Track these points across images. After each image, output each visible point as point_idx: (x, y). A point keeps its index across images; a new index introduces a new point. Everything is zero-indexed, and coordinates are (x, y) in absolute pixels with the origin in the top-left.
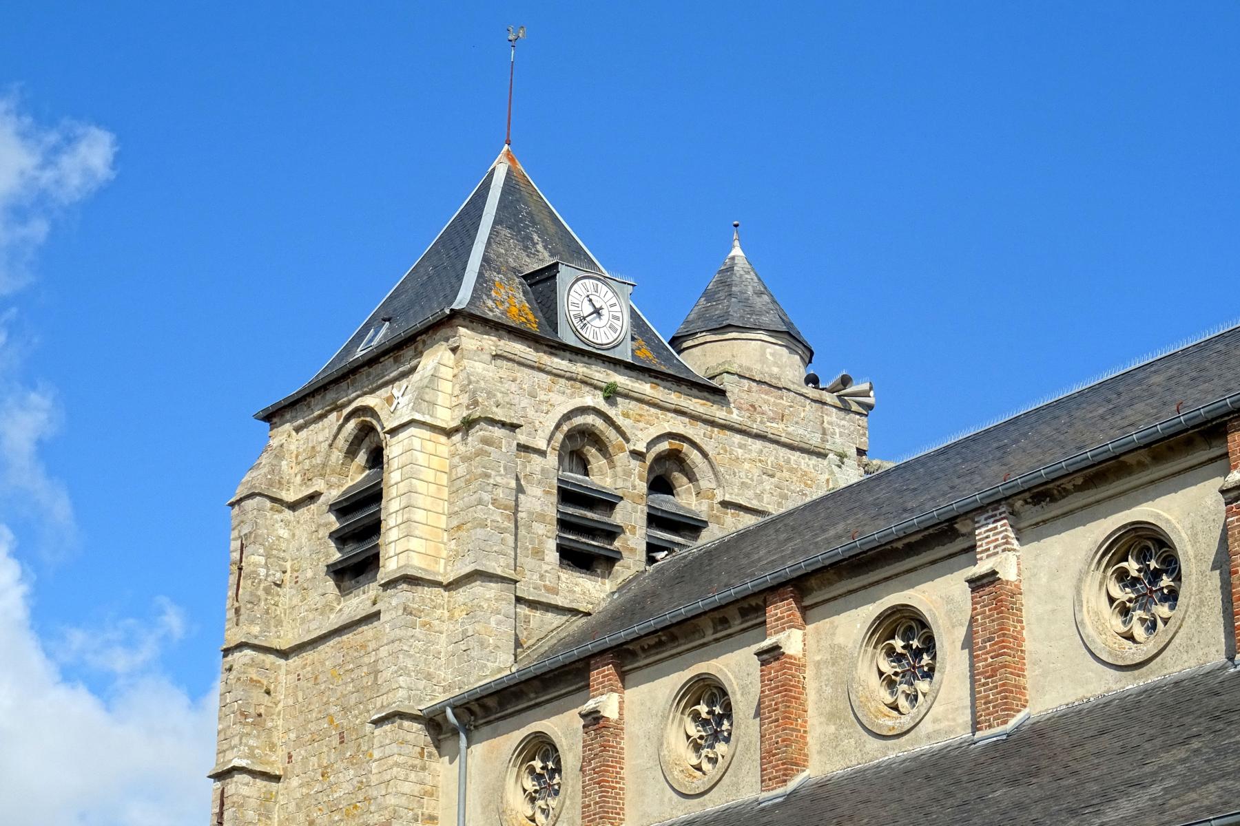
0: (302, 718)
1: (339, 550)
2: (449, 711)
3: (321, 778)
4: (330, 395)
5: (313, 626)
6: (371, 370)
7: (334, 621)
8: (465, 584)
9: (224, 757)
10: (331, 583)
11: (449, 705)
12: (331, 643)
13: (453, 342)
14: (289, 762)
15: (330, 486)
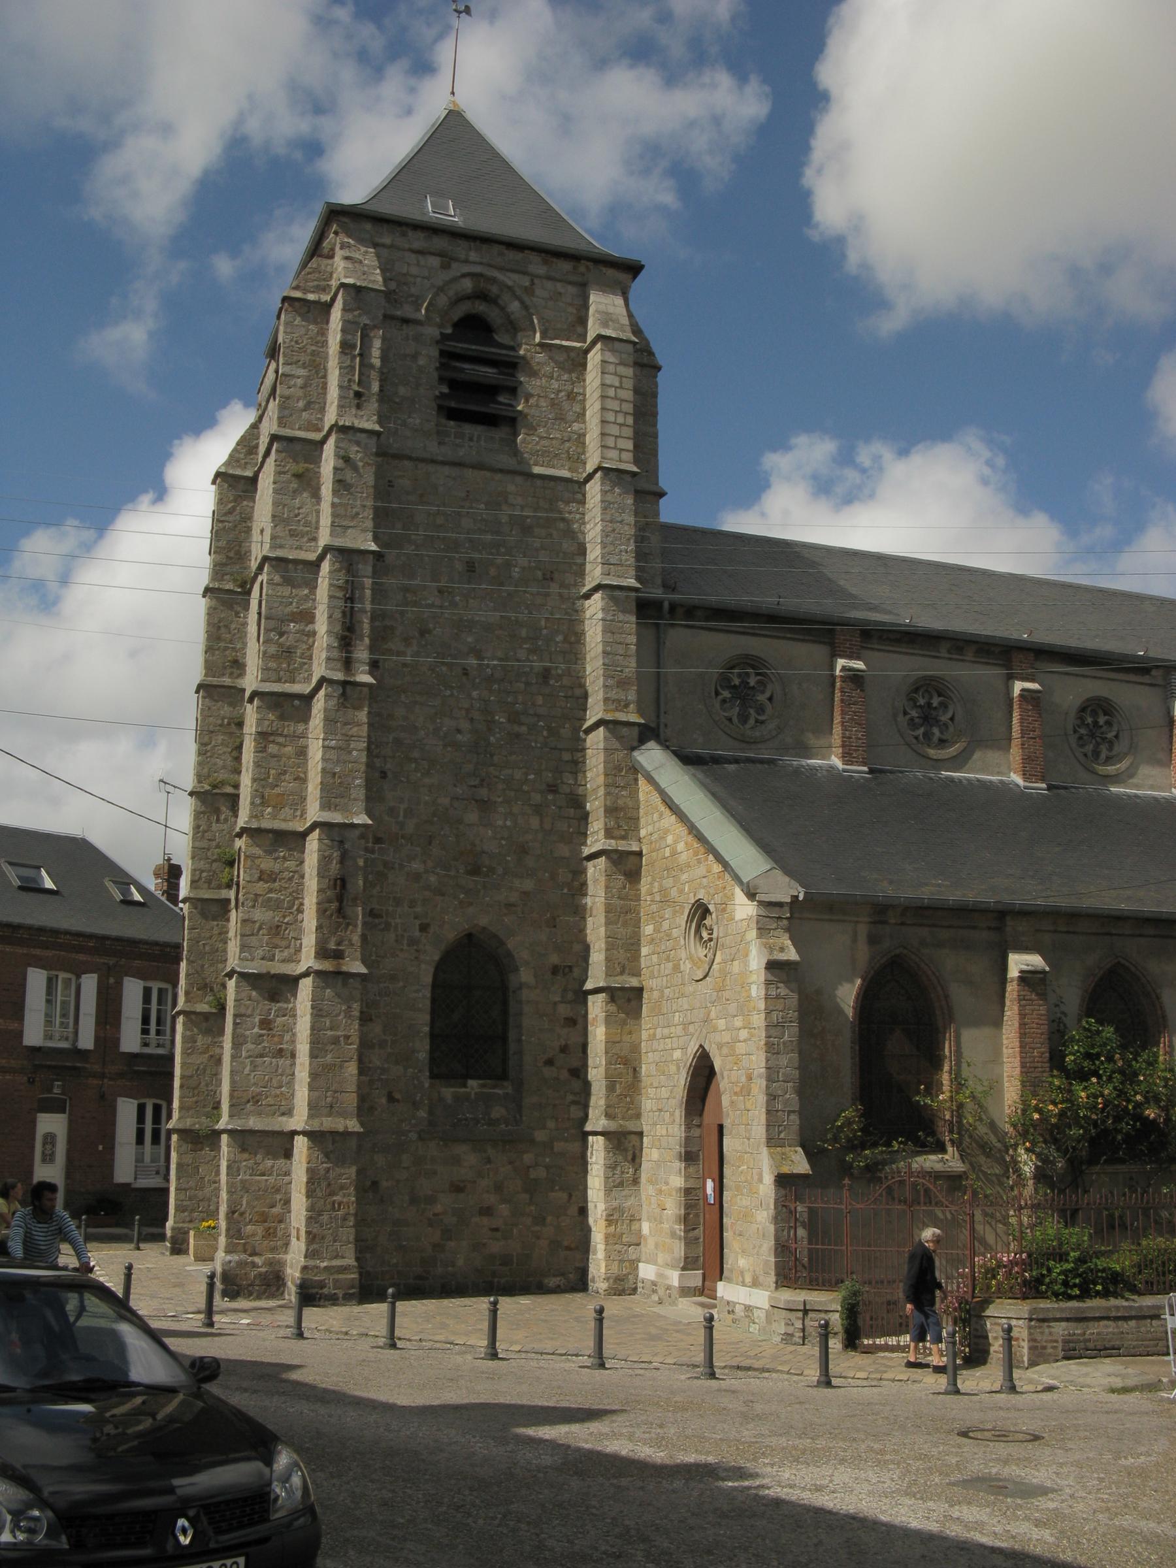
6: (506, 251)
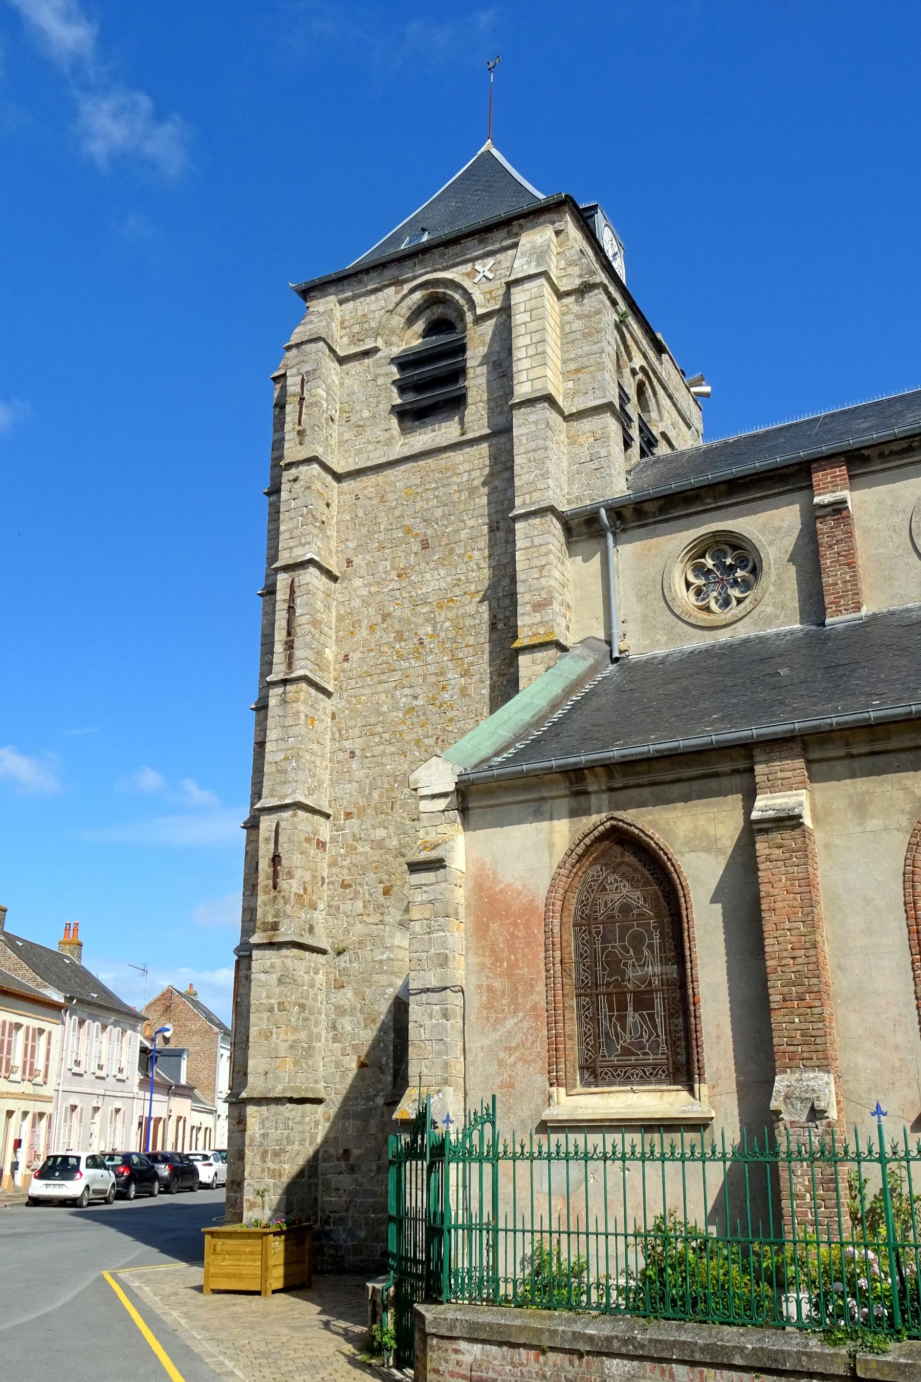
0: (364, 530)
1: (400, 397)
2: (603, 512)
3: (396, 578)
4: (390, 273)
5: (372, 455)
6: (446, 251)
7: (397, 452)
8: (591, 415)
9: (291, 552)
10: (394, 421)
11: (603, 506)
12: (403, 468)
13: (559, 226)
14: (348, 567)
15: (388, 344)
